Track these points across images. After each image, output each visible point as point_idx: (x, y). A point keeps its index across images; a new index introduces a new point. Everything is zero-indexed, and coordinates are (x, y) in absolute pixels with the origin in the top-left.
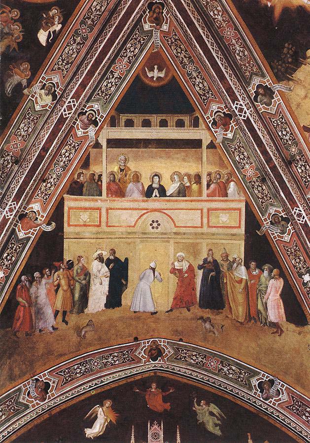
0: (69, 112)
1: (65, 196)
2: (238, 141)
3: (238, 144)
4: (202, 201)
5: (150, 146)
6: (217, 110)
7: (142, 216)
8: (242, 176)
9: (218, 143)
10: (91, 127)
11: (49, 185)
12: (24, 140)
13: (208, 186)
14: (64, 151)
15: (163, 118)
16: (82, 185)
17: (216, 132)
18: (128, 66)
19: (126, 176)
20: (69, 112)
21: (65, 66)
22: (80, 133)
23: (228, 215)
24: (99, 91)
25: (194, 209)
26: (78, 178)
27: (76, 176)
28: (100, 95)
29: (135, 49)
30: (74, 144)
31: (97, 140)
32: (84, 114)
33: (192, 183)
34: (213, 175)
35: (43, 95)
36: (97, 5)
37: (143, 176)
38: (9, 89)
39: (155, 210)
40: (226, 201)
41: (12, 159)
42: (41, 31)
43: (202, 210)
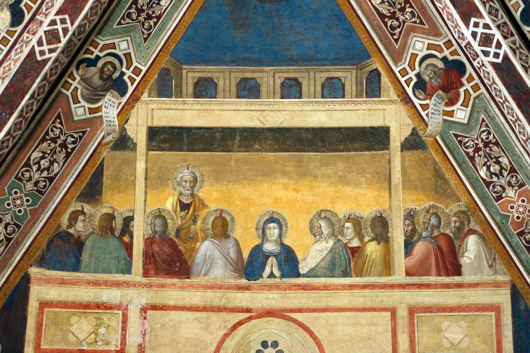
1: (34, 271)
2: (483, 129)
3: (484, 136)
4: (392, 286)
5: (257, 147)
6: (426, 52)
7: (235, 327)
8: (498, 219)
9: (430, 136)
10: (108, 96)
13: (409, 245)
14: (36, 155)
15: (287, 75)
17: (425, 107)
19: (195, 222)
22: (80, 111)
23: (464, 324)
25: (374, 310)
26: (70, 226)
27: (65, 220)
28: (134, 16)
30: (63, 138)
32: (93, 63)
33: (367, 239)
34: (421, 219)
37: (239, 220)
39: (270, 313)
40: (459, 286)
43: (393, 312)
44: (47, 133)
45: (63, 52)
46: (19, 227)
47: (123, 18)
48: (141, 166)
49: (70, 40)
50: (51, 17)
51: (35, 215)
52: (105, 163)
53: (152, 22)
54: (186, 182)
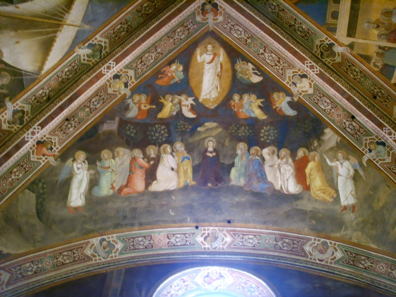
0: (315, 68)
10: (334, 49)
11: (379, 94)
12: (336, 107)
16: (385, 65)
18: (286, 12)
19: (384, 24)
20: (315, 68)
21: (281, 64)
24: (304, 39)
26: (378, 67)
27: (376, 69)
28: (307, 38)
29: (273, 5)
30: (347, 66)
31: (347, 46)
35: (301, 85)
36: (237, 33)
38: (290, 112)
41: (349, 121)
42: (251, 79)
44: (345, 71)
45: (317, 64)
46: (376, 85)
47: (308, 42)
48: (360, 41)
49: (314, 61)
50: (305, 67)
51: (373, 79)
52: (357, 53)
53: (310, 32)
54: (368, 25)
